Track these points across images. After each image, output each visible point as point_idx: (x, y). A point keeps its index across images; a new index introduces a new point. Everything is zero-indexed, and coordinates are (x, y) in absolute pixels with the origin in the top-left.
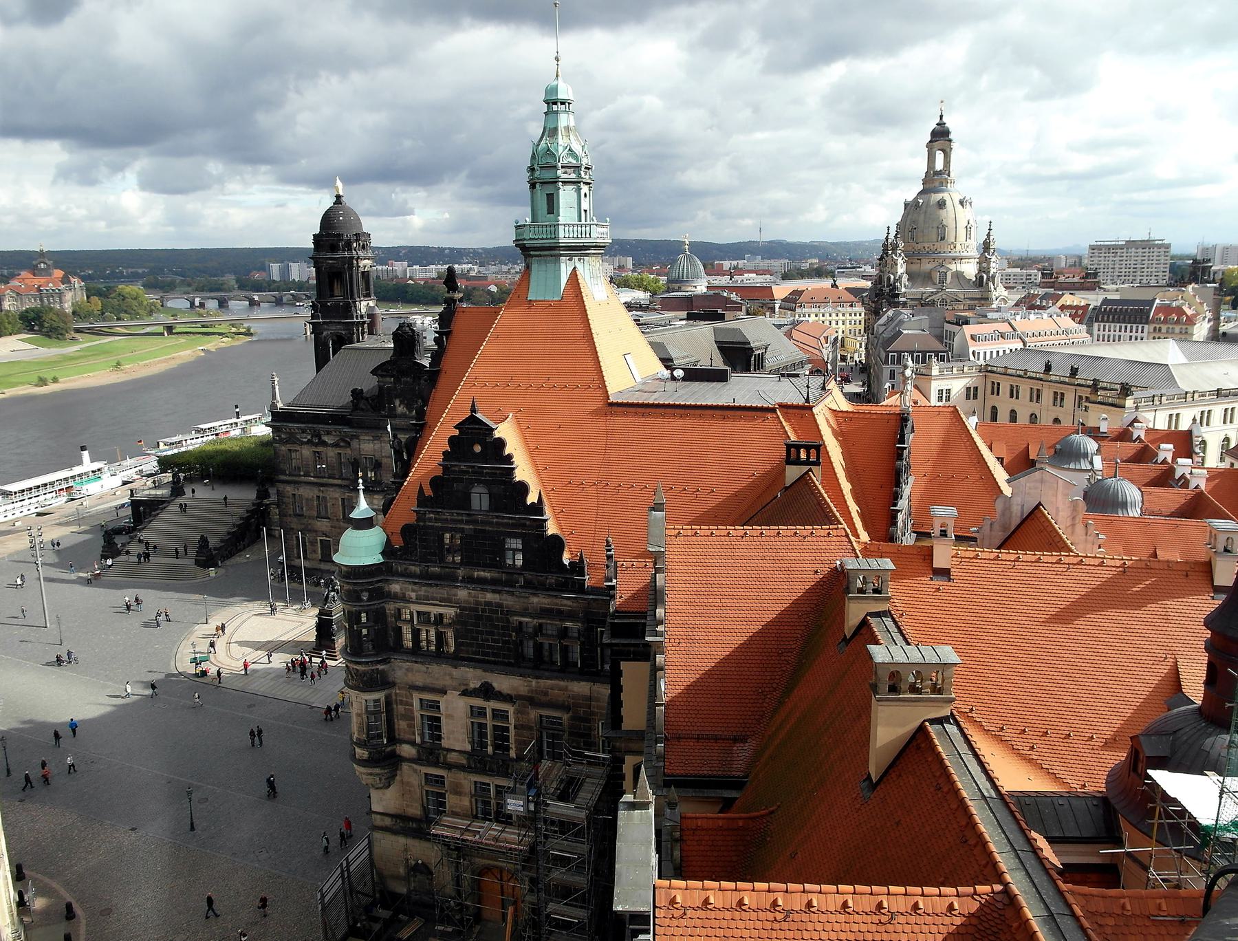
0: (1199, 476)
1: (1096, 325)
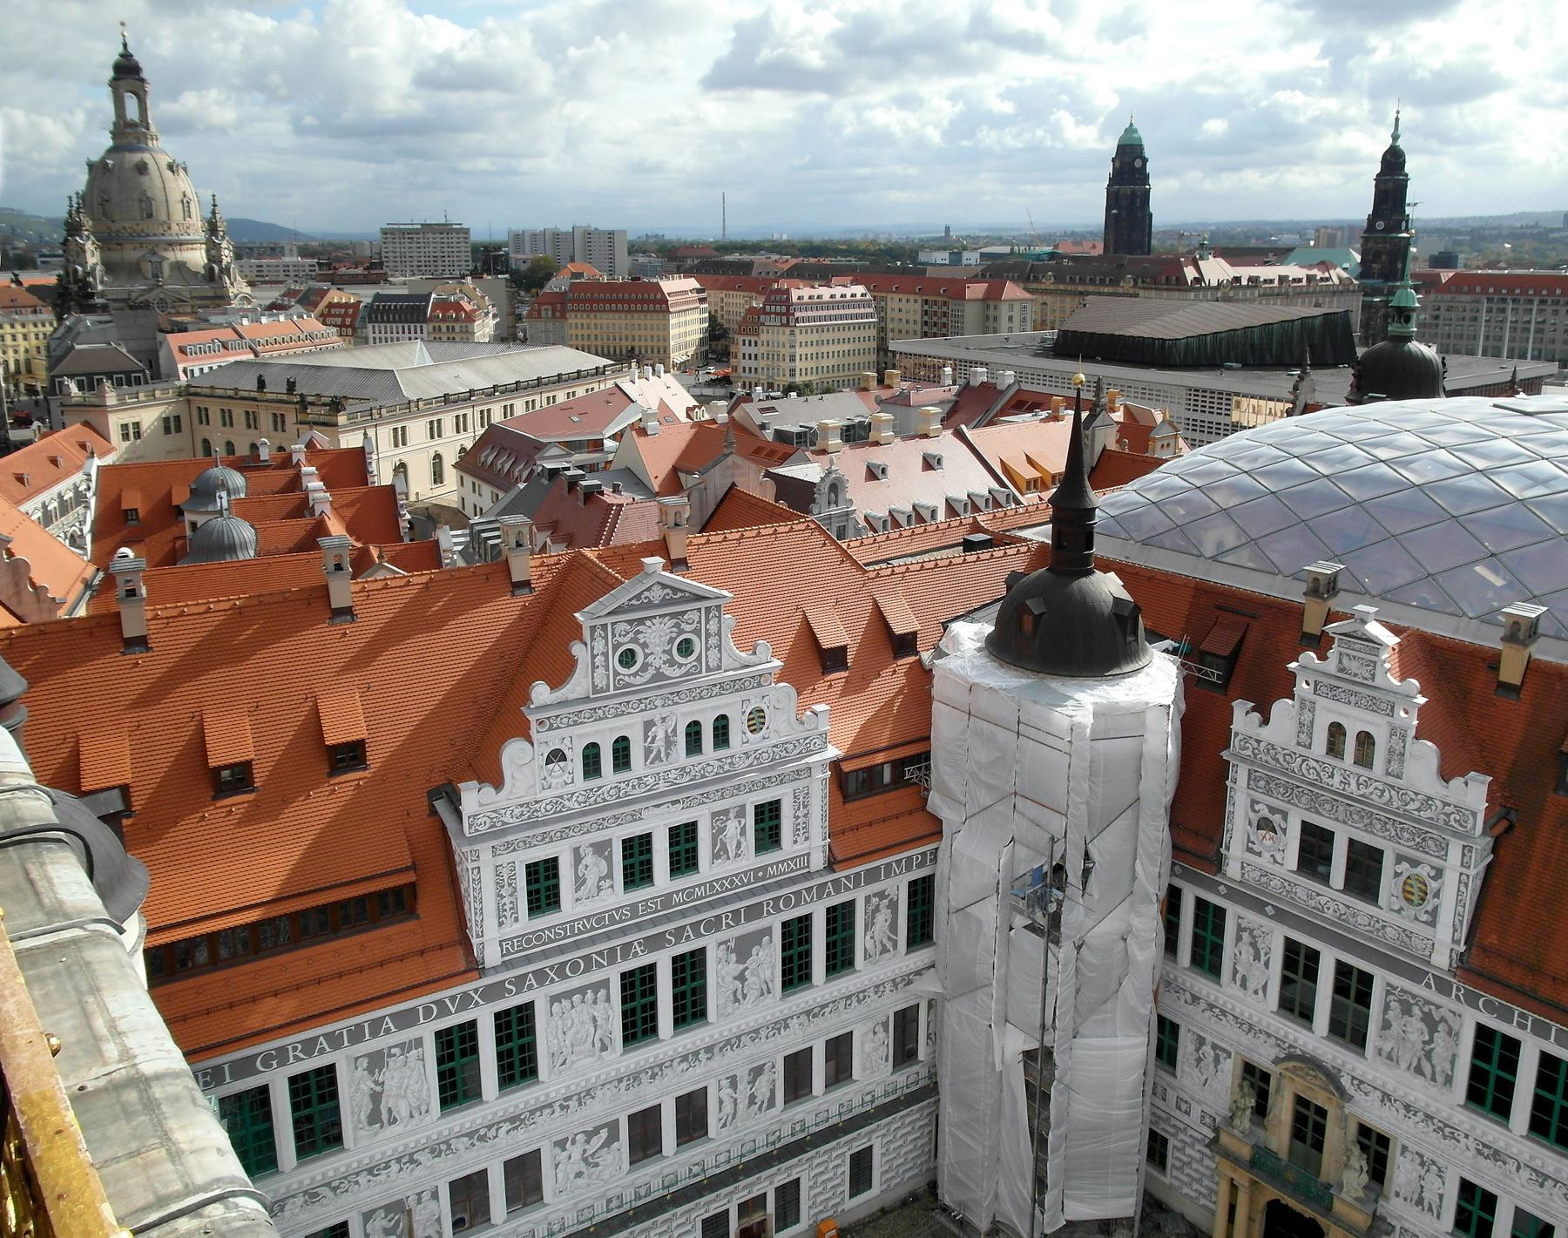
0: (322, 501)
1: (370, 326)
